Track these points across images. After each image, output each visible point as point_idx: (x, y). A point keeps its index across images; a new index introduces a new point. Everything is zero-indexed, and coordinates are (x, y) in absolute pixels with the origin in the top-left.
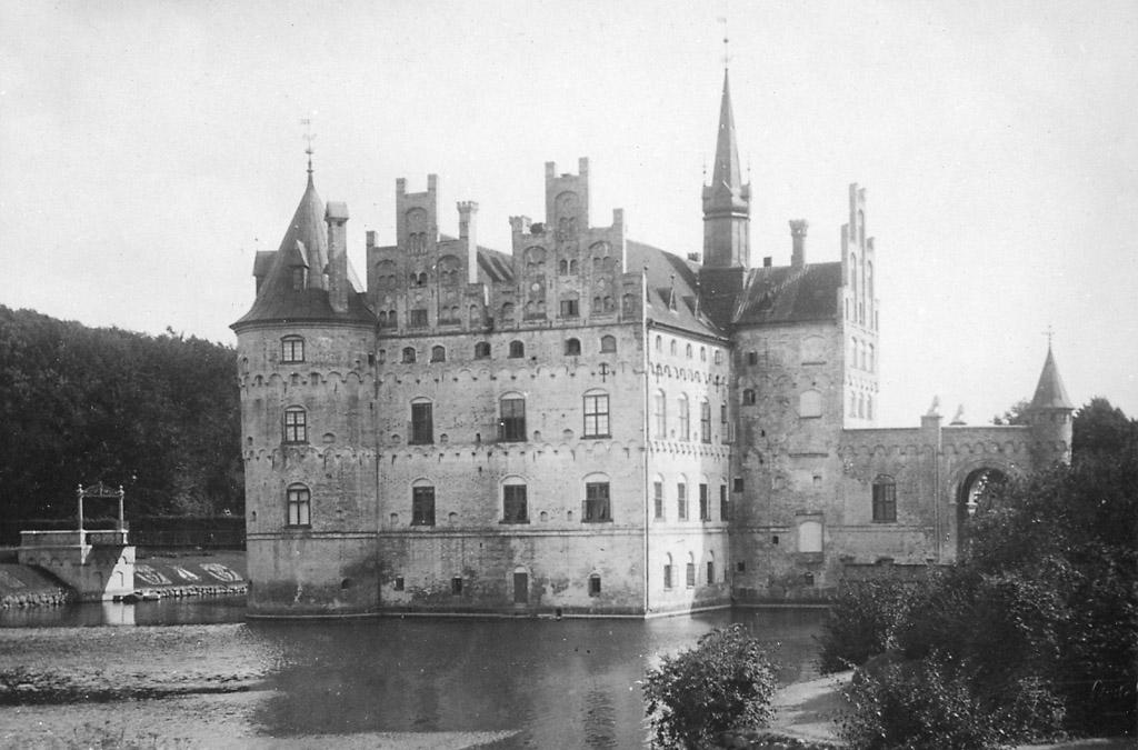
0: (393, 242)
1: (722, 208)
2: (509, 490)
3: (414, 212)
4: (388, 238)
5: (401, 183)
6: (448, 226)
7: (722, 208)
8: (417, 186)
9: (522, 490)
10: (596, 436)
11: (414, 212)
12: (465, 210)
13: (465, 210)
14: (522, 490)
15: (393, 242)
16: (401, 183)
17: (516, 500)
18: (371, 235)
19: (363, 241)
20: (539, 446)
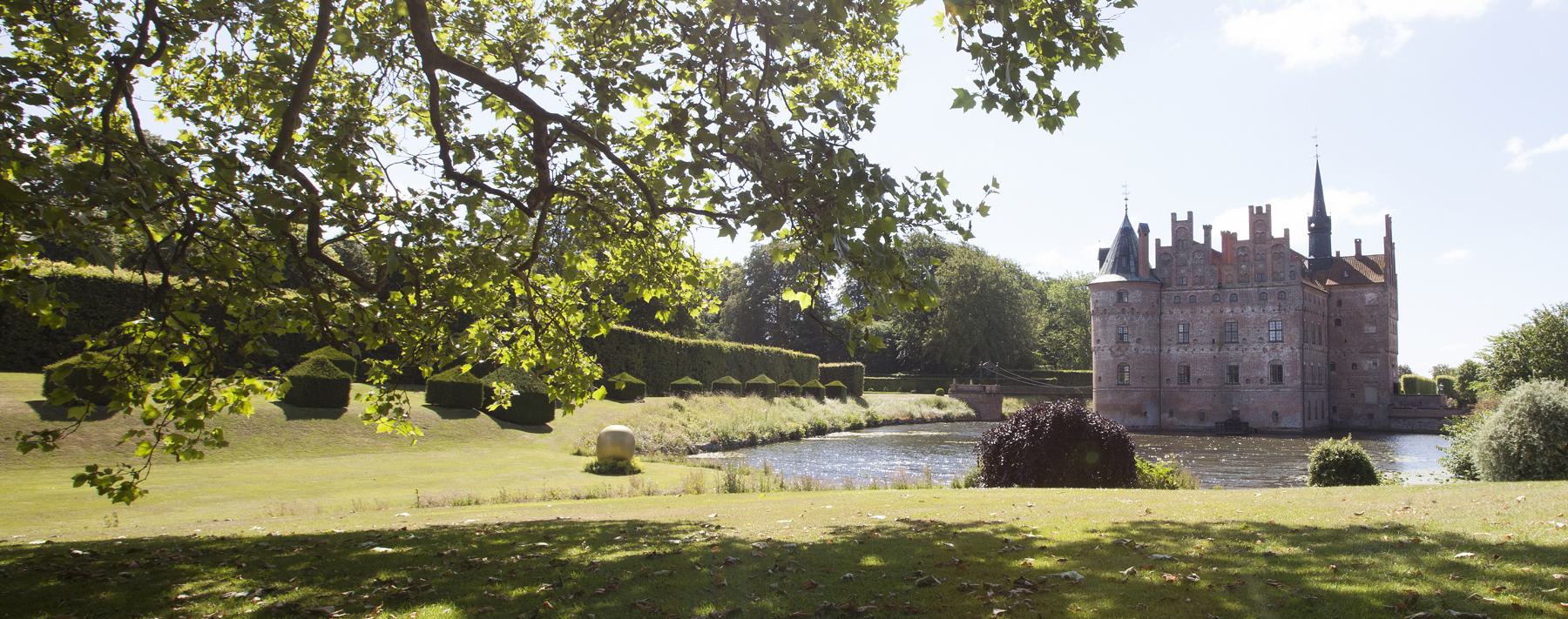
0: (1170, 245)
1: (1320, 226)
2: (1230, 368)
3: (1182, 229)
4: (1167, 242)
5: (1174, 215)
6: (1198, 237)
7: (1320, 226)
8: (1182, 217)
9: (1236, 368)
10: (1276, 341)
11: (1182, 229)
12: (1207, 229)
13: (1207, 229)
14: (1236, 368)
15: (1170, 245)
16: (1174, 215)
17: (1234, 373)
18: (1158, 241)
19: (1154, 242)
20: (1245, 347)
